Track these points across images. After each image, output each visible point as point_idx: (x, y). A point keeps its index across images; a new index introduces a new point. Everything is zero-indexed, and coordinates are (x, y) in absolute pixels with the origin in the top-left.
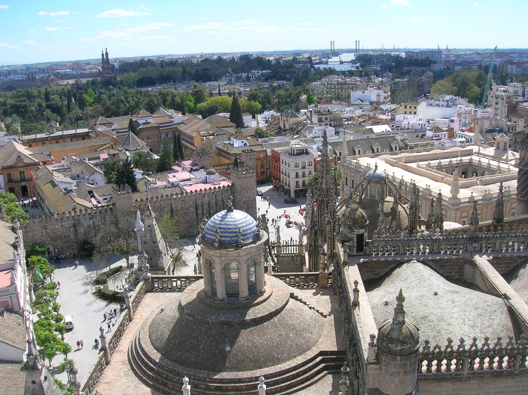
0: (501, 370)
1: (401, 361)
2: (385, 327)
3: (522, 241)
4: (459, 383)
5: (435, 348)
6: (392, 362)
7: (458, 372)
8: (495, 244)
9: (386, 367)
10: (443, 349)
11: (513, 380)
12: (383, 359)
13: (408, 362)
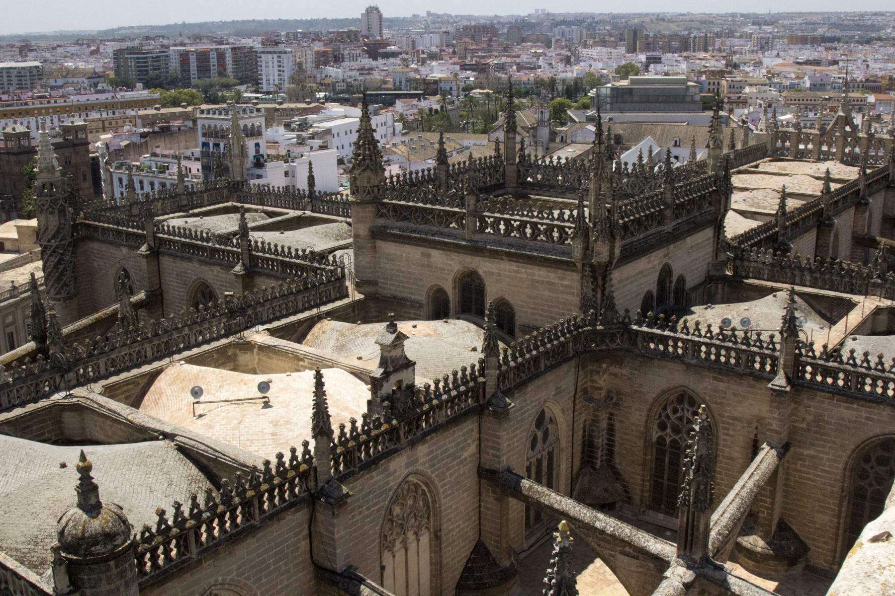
0: (237, 529)
1: (117, 566)
2: (71, 524)
3: (137, 349)
4: (188, 575)
5: (143, 533)
6: (103, 576)
7: (184, 558)
8: (99, 367)
9: (94, 590)
10: (154, 530)
11: (255, 539)
12: (86, 577)
13: (127, 565)
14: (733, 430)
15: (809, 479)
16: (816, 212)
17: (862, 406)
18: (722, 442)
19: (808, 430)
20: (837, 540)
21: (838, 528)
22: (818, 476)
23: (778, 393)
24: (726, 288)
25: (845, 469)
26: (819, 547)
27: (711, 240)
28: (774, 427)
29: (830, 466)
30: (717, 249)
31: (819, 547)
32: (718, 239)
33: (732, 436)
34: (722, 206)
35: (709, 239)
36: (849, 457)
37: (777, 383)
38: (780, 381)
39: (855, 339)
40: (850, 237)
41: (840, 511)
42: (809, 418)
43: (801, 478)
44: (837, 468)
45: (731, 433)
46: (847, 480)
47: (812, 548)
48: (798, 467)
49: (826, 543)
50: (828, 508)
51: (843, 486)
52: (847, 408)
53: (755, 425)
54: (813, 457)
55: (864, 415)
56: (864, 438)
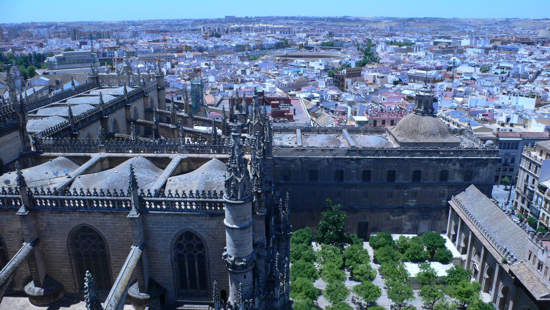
14: (11, 238)
15: (53, 253)
16: (98, 113)
17: (66, 214)
18: (8, 245)
19: (46, 230)
20: (74, 279)
21: (73, 273)
22: (57, 251)
23: (23, 217)
24: (33, 159)
25: (68, 245)
26: (68, 284)
27: (19, 137)
28: (26, 233)
29: (61, 245)
30: (24, 141)
31: (68, 284)
32: (24, 136)
33: (12, 241)
34: (21, 120)
35: (17, 137)
36: (68, 239)
37: (20, 212)
38: (22, 210)
39: (79, 178)
40: (125, 121)
41: (72, 265)
42: (45, 224)
43: (49, 253)
44: (64, 245)
45: (11, 239)
46: (70, 249)
47: (65, 285)
48: (47, 249)
49: (71, 281)
50: (66, 265)
51: (69, 253)
52: (60, 216)
53: (21, 233)
54: (51, 242)
55: (68, 218)
56: (71, 228)
